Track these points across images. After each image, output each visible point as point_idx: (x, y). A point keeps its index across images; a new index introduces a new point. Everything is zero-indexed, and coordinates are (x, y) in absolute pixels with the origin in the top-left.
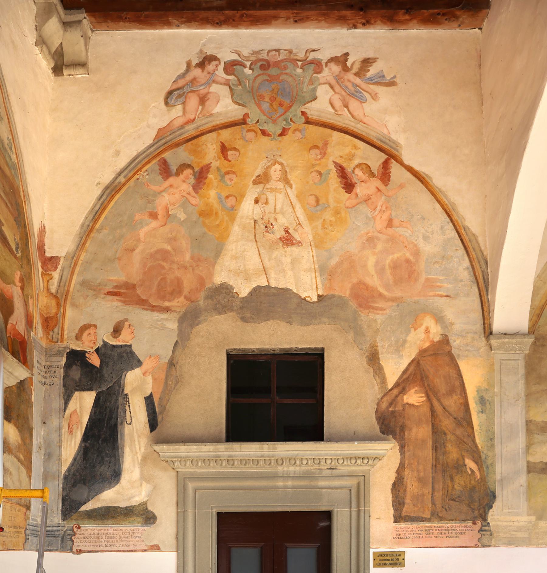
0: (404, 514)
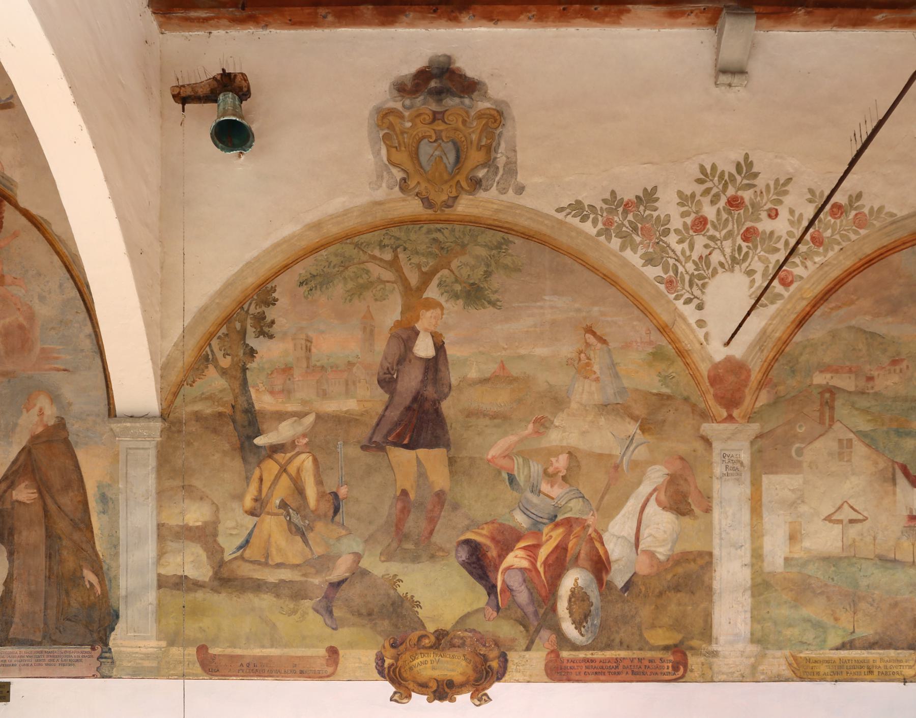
0: (11, 636)
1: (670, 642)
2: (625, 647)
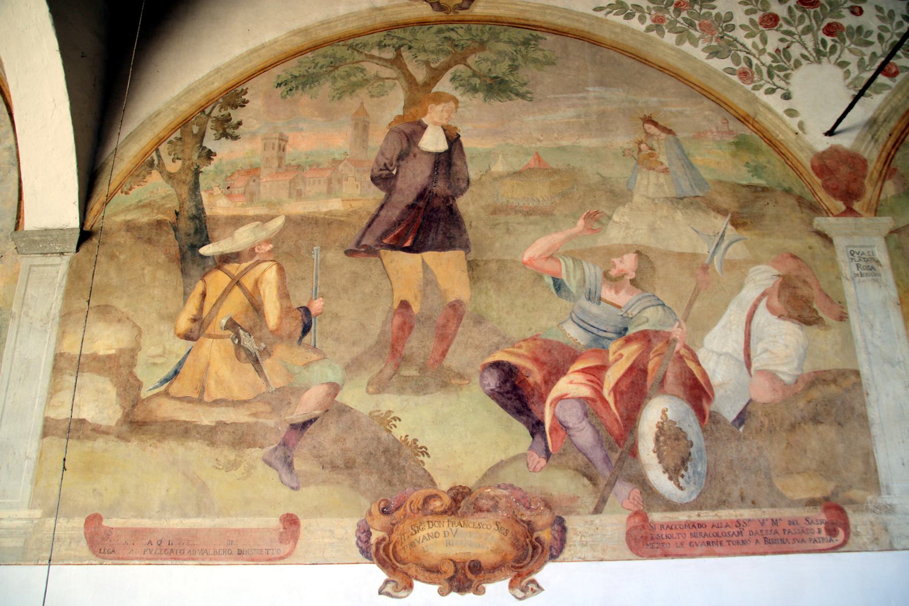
1: (818, 495)
2: (749, 503)
